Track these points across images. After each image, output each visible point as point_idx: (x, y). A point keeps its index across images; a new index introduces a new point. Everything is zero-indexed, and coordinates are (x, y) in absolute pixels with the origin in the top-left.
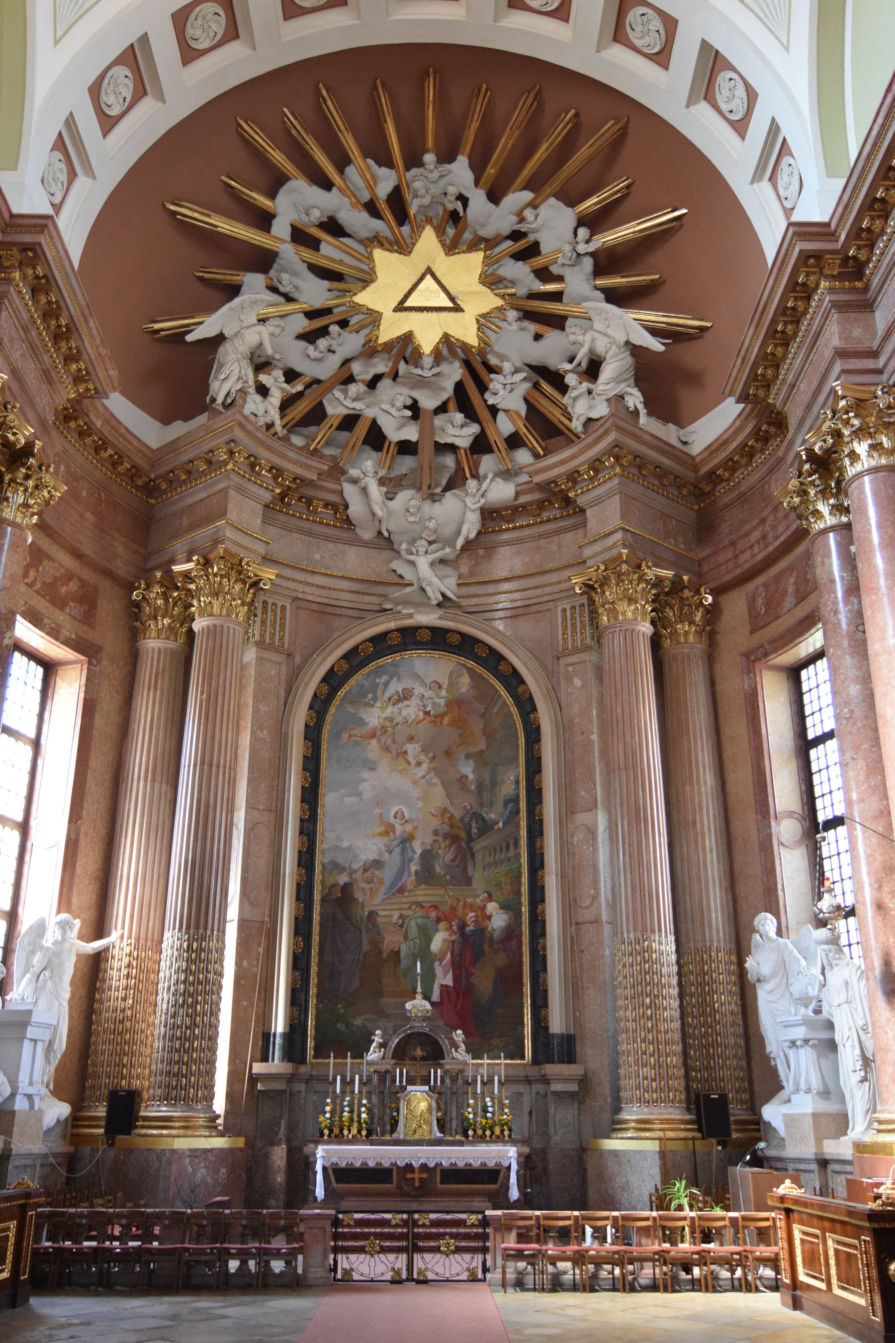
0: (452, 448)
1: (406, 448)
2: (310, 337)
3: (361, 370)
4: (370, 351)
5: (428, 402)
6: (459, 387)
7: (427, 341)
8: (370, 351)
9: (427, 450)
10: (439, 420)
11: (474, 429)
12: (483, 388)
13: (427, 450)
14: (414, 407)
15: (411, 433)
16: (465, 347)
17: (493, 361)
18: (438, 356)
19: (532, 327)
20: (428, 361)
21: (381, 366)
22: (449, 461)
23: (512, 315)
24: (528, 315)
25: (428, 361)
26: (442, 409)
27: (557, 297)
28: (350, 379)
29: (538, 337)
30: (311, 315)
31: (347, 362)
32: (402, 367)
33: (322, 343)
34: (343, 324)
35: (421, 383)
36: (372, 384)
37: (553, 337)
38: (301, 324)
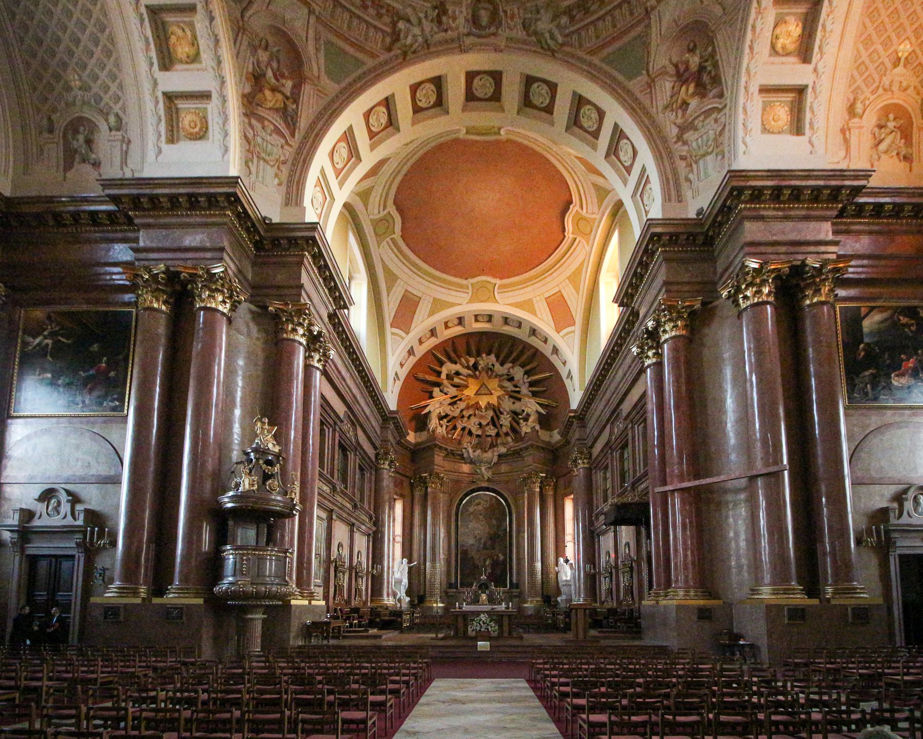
1: (478, 436)
4: (468, 408)
5: (484, 423)
6: (492, 418)
7: (483, 404)
10: (487, 428)
11: (496, 430)
12: (498, 418)
14: (480, 424)
15: (480, 433)
18: (486, 408)
19: (512, 400)
21: (471, 412)
22: (489, 439)
24: (511, 397)
26: (488, 424)
27: (519, 392)
28: (463, 417)
30: (452, 398)
31: (462, 411)
34: (460, 400)
35: (482, 417)
36: (469, 417)
37: (518, 404)
38: (449, 401)
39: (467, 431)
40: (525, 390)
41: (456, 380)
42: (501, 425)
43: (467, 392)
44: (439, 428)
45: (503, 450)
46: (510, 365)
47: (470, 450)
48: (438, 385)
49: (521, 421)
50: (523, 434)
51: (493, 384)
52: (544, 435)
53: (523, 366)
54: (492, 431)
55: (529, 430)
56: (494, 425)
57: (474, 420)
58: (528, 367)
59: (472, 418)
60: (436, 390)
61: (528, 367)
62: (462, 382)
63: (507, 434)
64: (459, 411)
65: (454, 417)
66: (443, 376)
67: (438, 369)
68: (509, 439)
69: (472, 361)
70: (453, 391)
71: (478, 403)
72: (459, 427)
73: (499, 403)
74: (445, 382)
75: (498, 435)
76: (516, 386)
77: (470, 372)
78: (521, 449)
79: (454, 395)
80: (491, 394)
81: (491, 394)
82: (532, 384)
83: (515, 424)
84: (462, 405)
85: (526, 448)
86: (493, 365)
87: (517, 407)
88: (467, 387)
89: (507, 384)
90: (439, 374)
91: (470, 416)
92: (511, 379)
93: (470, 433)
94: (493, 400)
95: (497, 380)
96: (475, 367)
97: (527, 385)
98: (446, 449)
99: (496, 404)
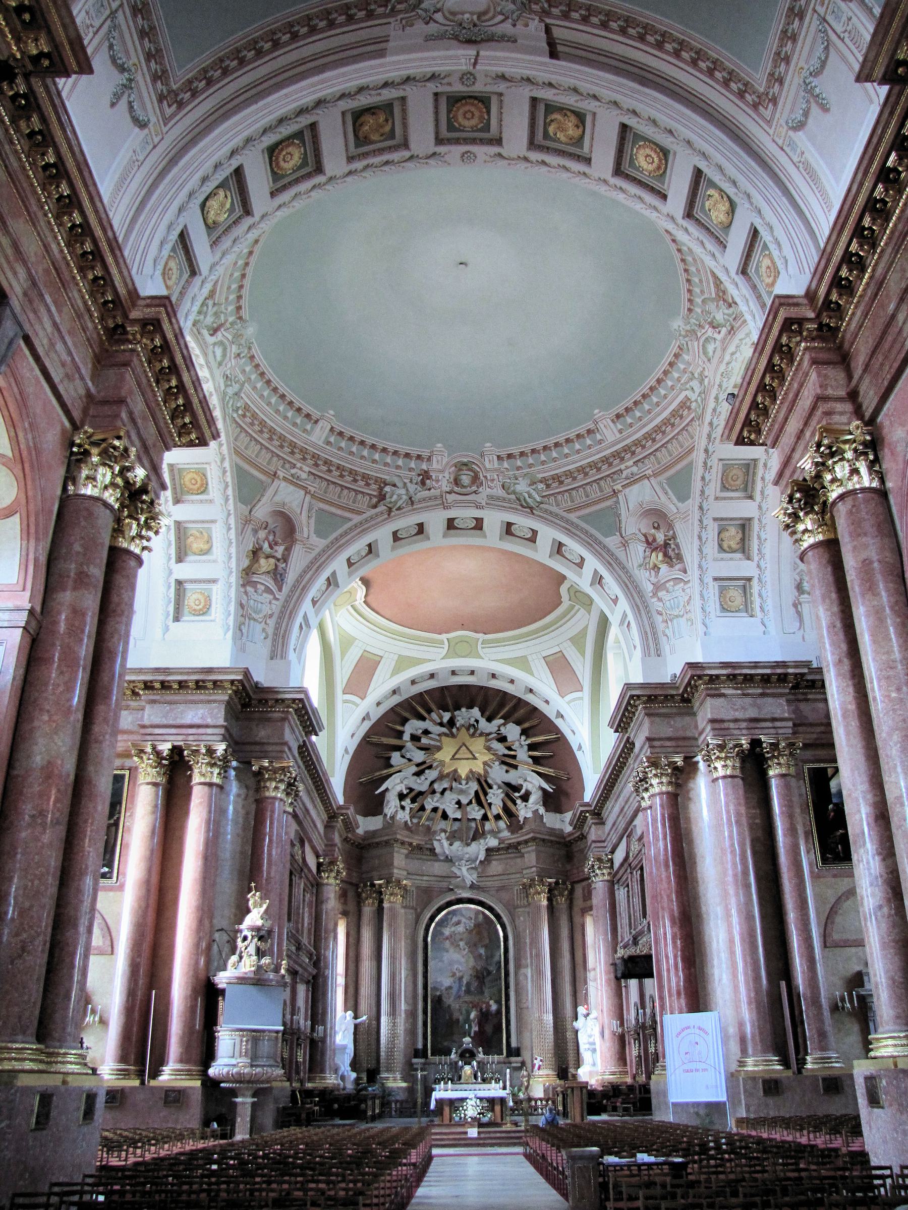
0: (474, 819)
1: (455, 820)
2: (418, 774)
3: (438, 787)
4: (441, 777)
5: (465, 801)
6: (476, 792)
7: (463, 772)
8: (441, 777)
9: (464, 821)
10: (469, 808)
11: (482, 812)
12: (486, 794)
13: (464, 821)
14: (459, 803)
15: (458, 815)
16: (479, 775)
17: (490, 781)
18: (468, 779)
19: (505, 768)
20: (464, 782)
21: (446, 785)
22: (473, 825)
23: (497, 763)
24: (503, 763)
25: (464, 782)
26: (470, 802)
27: (514, 757)
28: (434, 792)
29: (507, 771)
30: (418, 765)
31: (432, 783)
32: (454, 784)
33: (423, 778)
34: (430, 767)
35: (462, 792)
36: (443, 793)
37: (513, 772)
38: (414, 769)
39: (440, 813)
40: (523, 755)
41: (424, 741)
42: (490, 804)
43: (439, 756)
44: (400, 812)
45: (493, 842)
46: (502, 721)
47: (446, 843)
48: (399, 748)
49: (519, 801)
50: (521, 819)
51: (477, 745)
52: (552, 820)
53: (518, 723)
54: (476, 813)
55: (530, 815)
56: (480, 803)
57: (451, 797)
58: (526, 725)
59: (447, 793)
60: (396, 757)
61: (526, 725)
62: (432, 743)
63: (498, 817)
64: (428, 783)
65: (421, 793)
66: (406, 737)
67: (399, 728)
68: (502, 824)
69: (447, 716)
70: (419, 756)
71: (456, 771)
72: (429, 808)
73: (486, 772)
74: (409, 745)
75: (485, 818)
76: (509, 749)
77: (444, 730)
78: (519, 843)
79: (420, 760)
80: (475, 758)
81: (475, 758)
82: (531, 747)
83: (510, 804)
84: (431, 775)
85: (526, 842)
86: (477, 721)
87: (513, 777)
88: (439, 749)
89: (500, 748)
90: (400, 734)
91: (445, 790)
92: (502, 739)
93: (445, 816)
94: (478, 768)
95: (483, 739)
96: (452, 723)
97: (526, 748)
98: (410, 844)
99: (482, 772)
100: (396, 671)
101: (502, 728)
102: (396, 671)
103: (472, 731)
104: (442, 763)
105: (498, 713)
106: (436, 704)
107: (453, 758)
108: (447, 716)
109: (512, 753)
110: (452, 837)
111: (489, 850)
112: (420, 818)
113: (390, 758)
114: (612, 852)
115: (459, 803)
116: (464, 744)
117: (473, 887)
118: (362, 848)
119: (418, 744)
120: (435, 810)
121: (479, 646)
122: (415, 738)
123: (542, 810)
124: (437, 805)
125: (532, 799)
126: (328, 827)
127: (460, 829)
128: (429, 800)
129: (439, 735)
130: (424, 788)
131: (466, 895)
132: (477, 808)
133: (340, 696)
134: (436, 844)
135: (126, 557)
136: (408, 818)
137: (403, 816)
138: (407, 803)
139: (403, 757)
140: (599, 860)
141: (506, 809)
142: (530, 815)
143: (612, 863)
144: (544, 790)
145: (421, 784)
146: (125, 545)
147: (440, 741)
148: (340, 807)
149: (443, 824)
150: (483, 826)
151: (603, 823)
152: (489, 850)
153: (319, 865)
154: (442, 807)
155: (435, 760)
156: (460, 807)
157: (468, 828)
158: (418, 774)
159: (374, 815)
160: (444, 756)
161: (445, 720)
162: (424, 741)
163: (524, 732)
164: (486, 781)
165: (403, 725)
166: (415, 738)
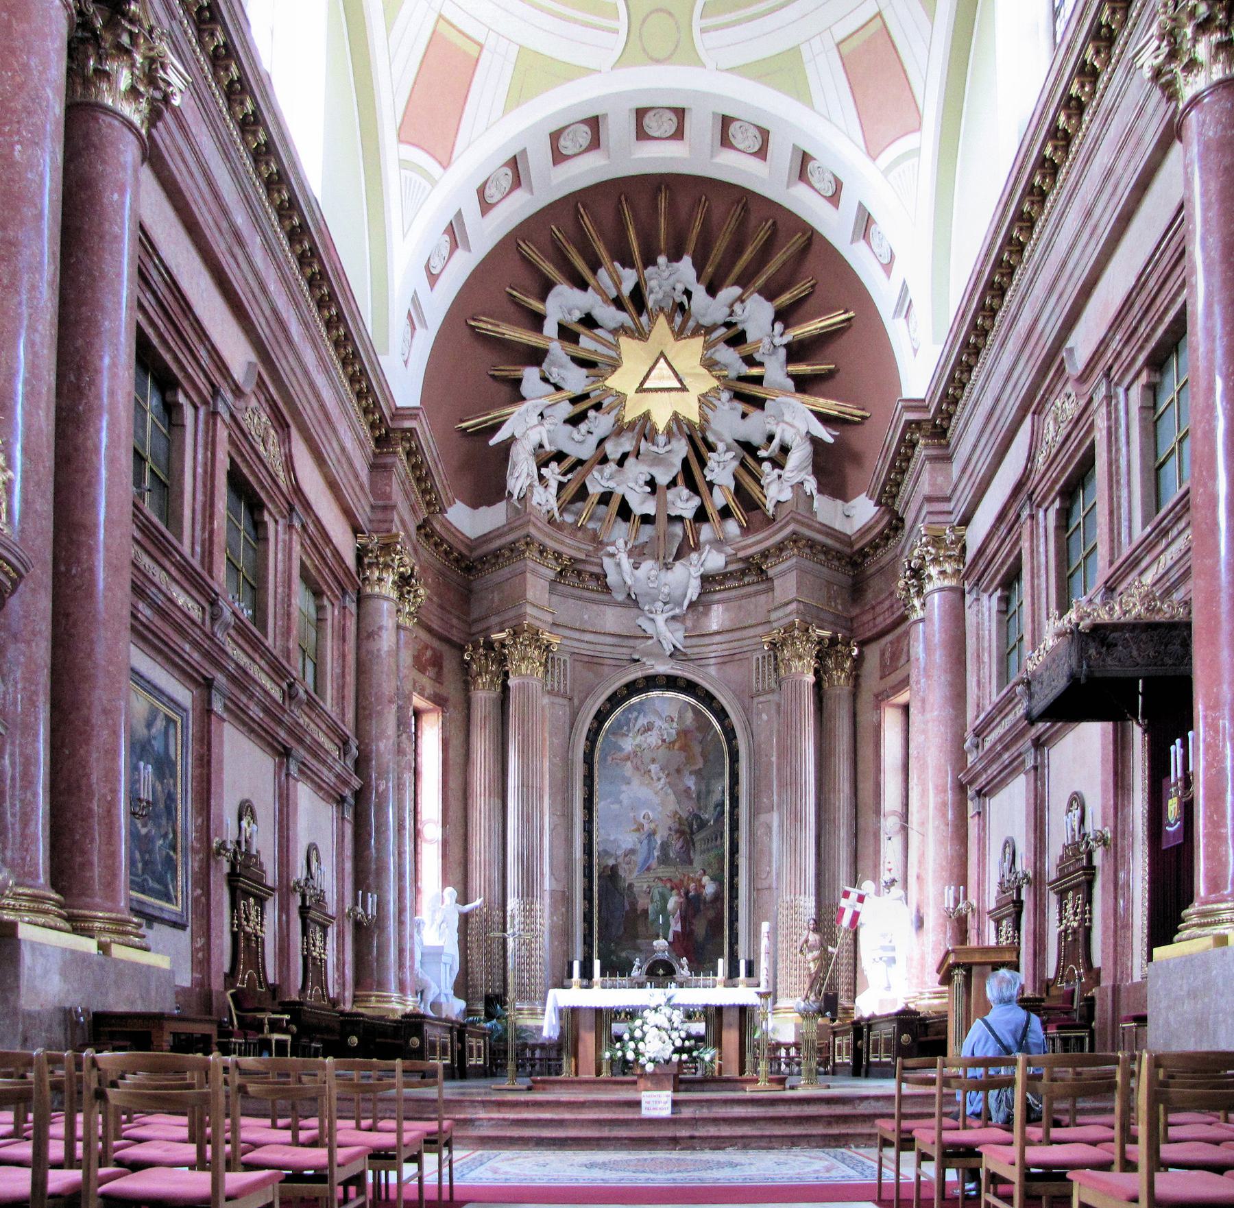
0: (680, 519)
1: (647, 519)
2: (575, 420)
3: (613, 450)
4: (619, 430)
5: (663, 479)
6: (685, 462)
7: (661, 420)
8: (619, 430)
9: (662, 521)
10: (670, 495)
11: (696, 501)
12: (703, 463)
13: (662, 521)
14: (651, 483)
15: (650, 508)
16: (690, 424)
17: (711, 438)
18: (669, 433)
19: (740, 407)
20: (662, 439)
21: (627, 445)
22: (678, 529)
23: (725, 396)
24: (739, 396)
25: (662, 439)
26: (673, 483)
27: (758, 380)
28: (604, 460)
29: (744, 415)
30: (574, 401)
31: (601, 442)
32: (644, 445)
33: (583, 427)
34: (598, 407)
35: (657, 460)
36: (621, 462)
37: (755, 415)
38: (567, 410)
39: (615, 504)
40: (776, 371)
41: (586, 342)
42: (711, 485)
43: (615, 382)
44: (539, 489)
45: (715, 561)
46: (736, 291)
47: (626, 563)
48: (536, 356)
49: (766, 466)
50: (770, 506)
51: (689, 353)
52: (827, 510)
53: (769, 294)
54: (683, 503)
55: (787, 495)
56: (693, 487)
57: (637, 471)
58: (785, 299)
59: (630, 461)
60: (530, 375)
61: (785, 299)
62: (601, 349)
63: (725, 513)
64: (593, 441)
65: (580, 462)
66: (550, 328)
67: (535, 304)
68: (732, 527)
69: (629, 279)
70: (576, 381)
71: (646, 416)
72: (595, 490)
73: (704, 418)
74: (557, 349)
75: (701, 515)
76: (750, 361)
77: (623, 317)
78: (765, 555)
79: (579, 391)
80: (684, 389)
81: (684, 389)
82: (796, 352)
83: (748, 482)
84: (600, 423)
85: (780, 548)
86: (688, 293)
87: (754, 427)
88: (614, 365)
89: (729, 357)
90: (537, 321)
91: (625, 456)
92: (737, 339)
93: (625, 512)
94: (691, 412)
95: (698, 342)
96: (638, 295)
97: (782, 353)
98: (558, 556)
99: (696, 418)
100: (517, 97)
101: (738, 308)
102: (517, 97)
103: (678, 319)
104: (621, 398)
105: (726, 276)
106: (609, 251)
107: (641, 389)
108: (629, 279)
109: (755, 371)
110: (638, 553)
111: (706, 579)
112: (579, 514)
113: (518, 382)
114: (966, 521)
115: (651, 483)
116: (662, 355)
117: (675, 654)
118: (469, 569)
119: (571, 348)
120: (605, 498)
121: (697, 24)
122: (567, 334)
123: (811, 485)
124: (611, 484)
125: (793, 459)
126: (378, 467)
127: (654, 540)
128: (596, 474)
129: (614, 332)
130: (586, 451)
131: (663, 668)
132: (685, 492)
133: (393, 151)
134: (607, 562)
135: (105, 119)
136: (554, 504)
137: (545, 499)
138: (553, 472)
139: (545, 380)
140: (937, 541)
141: (740, 491)
142: (787, 495)
143: (964, 548)
144: (815, 441)
145: (580, 445)
146: (109, 101)
147: (617, 347)
148: (399, 414)
149: (621, 529)
150: (697, 533)
151: (948, 459)
152: (706, 579)
153: (361, 554)
154: (619, 490)
155: (607, 390)
156: (653, 492)
157: (669, 537)
158: (575, 420)
159: (490, 503)
160: (622, 381)
161: (627, 288)
162: (586, 342)
163: (784, 316)
164: (704, 439)
165: (543, 299)
166: (567, 334)
